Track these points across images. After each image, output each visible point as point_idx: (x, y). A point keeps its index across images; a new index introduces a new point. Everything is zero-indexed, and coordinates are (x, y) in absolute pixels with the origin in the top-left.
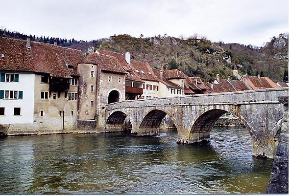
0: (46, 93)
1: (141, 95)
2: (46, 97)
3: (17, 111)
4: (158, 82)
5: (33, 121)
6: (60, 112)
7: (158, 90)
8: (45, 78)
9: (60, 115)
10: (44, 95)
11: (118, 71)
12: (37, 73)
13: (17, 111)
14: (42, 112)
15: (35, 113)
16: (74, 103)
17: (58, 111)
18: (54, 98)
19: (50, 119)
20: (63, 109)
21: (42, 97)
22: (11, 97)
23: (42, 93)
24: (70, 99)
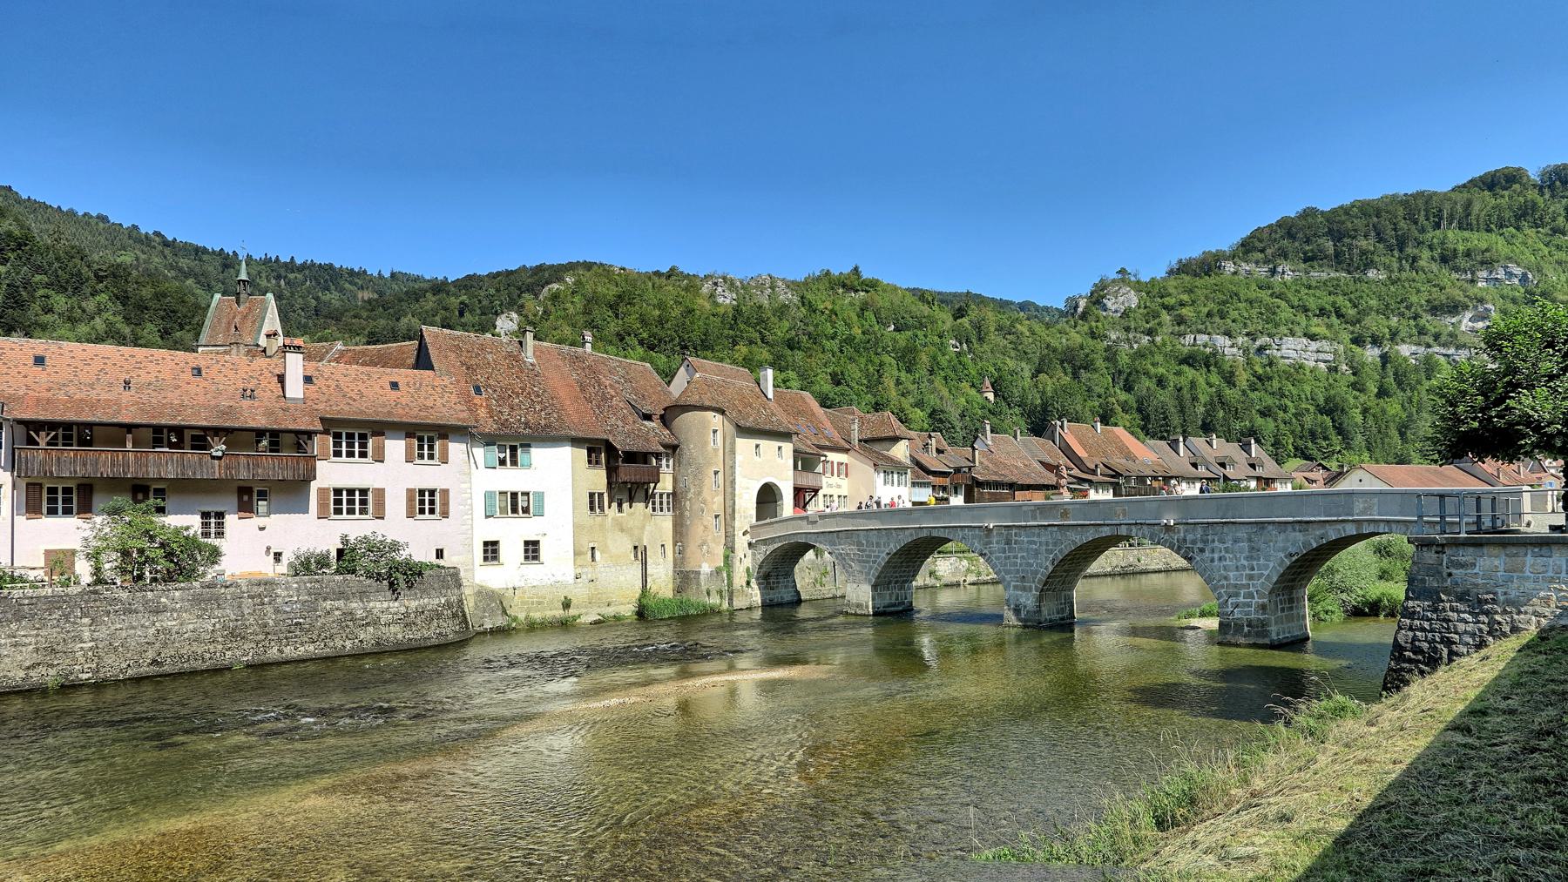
0: (601, 495)
1: (816, 491)
2: (601, 508)
3: (532, 550)
4: (846, 451)
5: (573, 576)
6: (636, 548)
7: (847, 475)
8: (600, 450)
9: (636, 556)
10: (594, 502)
11: (1471, 550)
12: (576, 442)
13: (532, 550)
14: (593, 548)
15: (577, 554)
16: (665, 522)
17: (631, 547)
18: (620, 510)
19: (613, 570)
20: (640, 540)
21: (592, 508)
22: (514, 510)
23: (591, 495)
24: (654, 509)
